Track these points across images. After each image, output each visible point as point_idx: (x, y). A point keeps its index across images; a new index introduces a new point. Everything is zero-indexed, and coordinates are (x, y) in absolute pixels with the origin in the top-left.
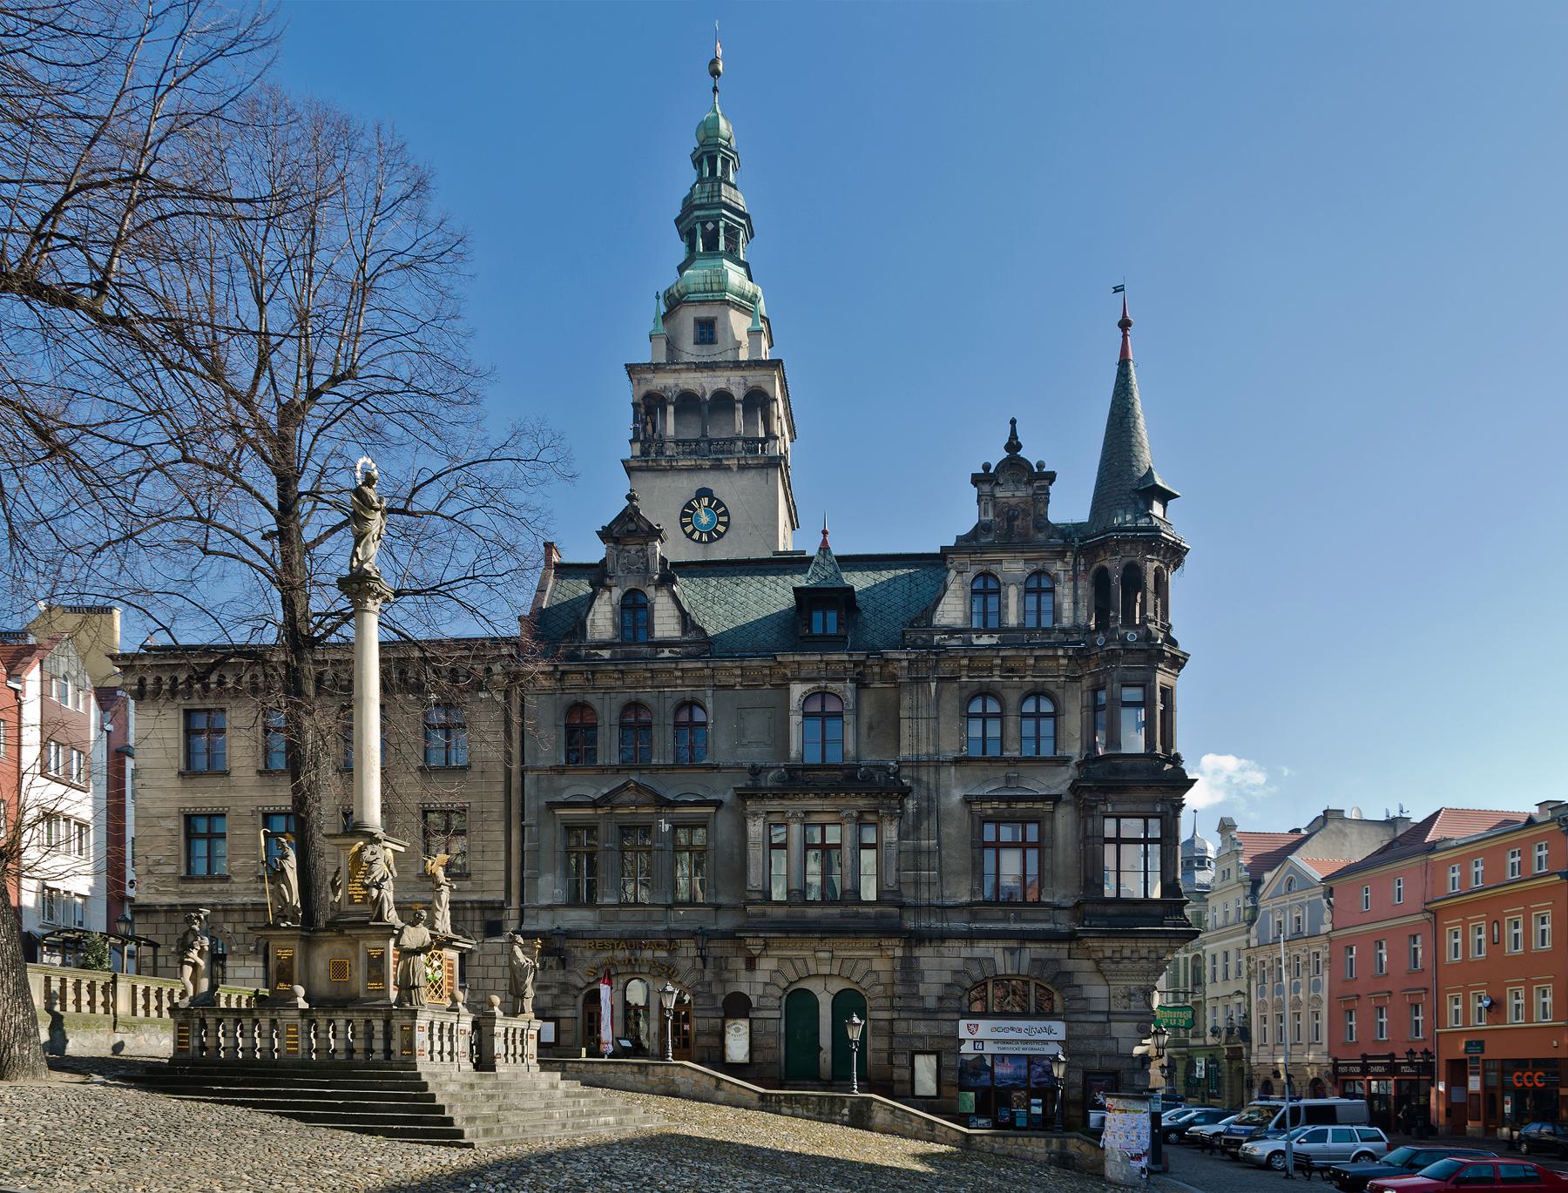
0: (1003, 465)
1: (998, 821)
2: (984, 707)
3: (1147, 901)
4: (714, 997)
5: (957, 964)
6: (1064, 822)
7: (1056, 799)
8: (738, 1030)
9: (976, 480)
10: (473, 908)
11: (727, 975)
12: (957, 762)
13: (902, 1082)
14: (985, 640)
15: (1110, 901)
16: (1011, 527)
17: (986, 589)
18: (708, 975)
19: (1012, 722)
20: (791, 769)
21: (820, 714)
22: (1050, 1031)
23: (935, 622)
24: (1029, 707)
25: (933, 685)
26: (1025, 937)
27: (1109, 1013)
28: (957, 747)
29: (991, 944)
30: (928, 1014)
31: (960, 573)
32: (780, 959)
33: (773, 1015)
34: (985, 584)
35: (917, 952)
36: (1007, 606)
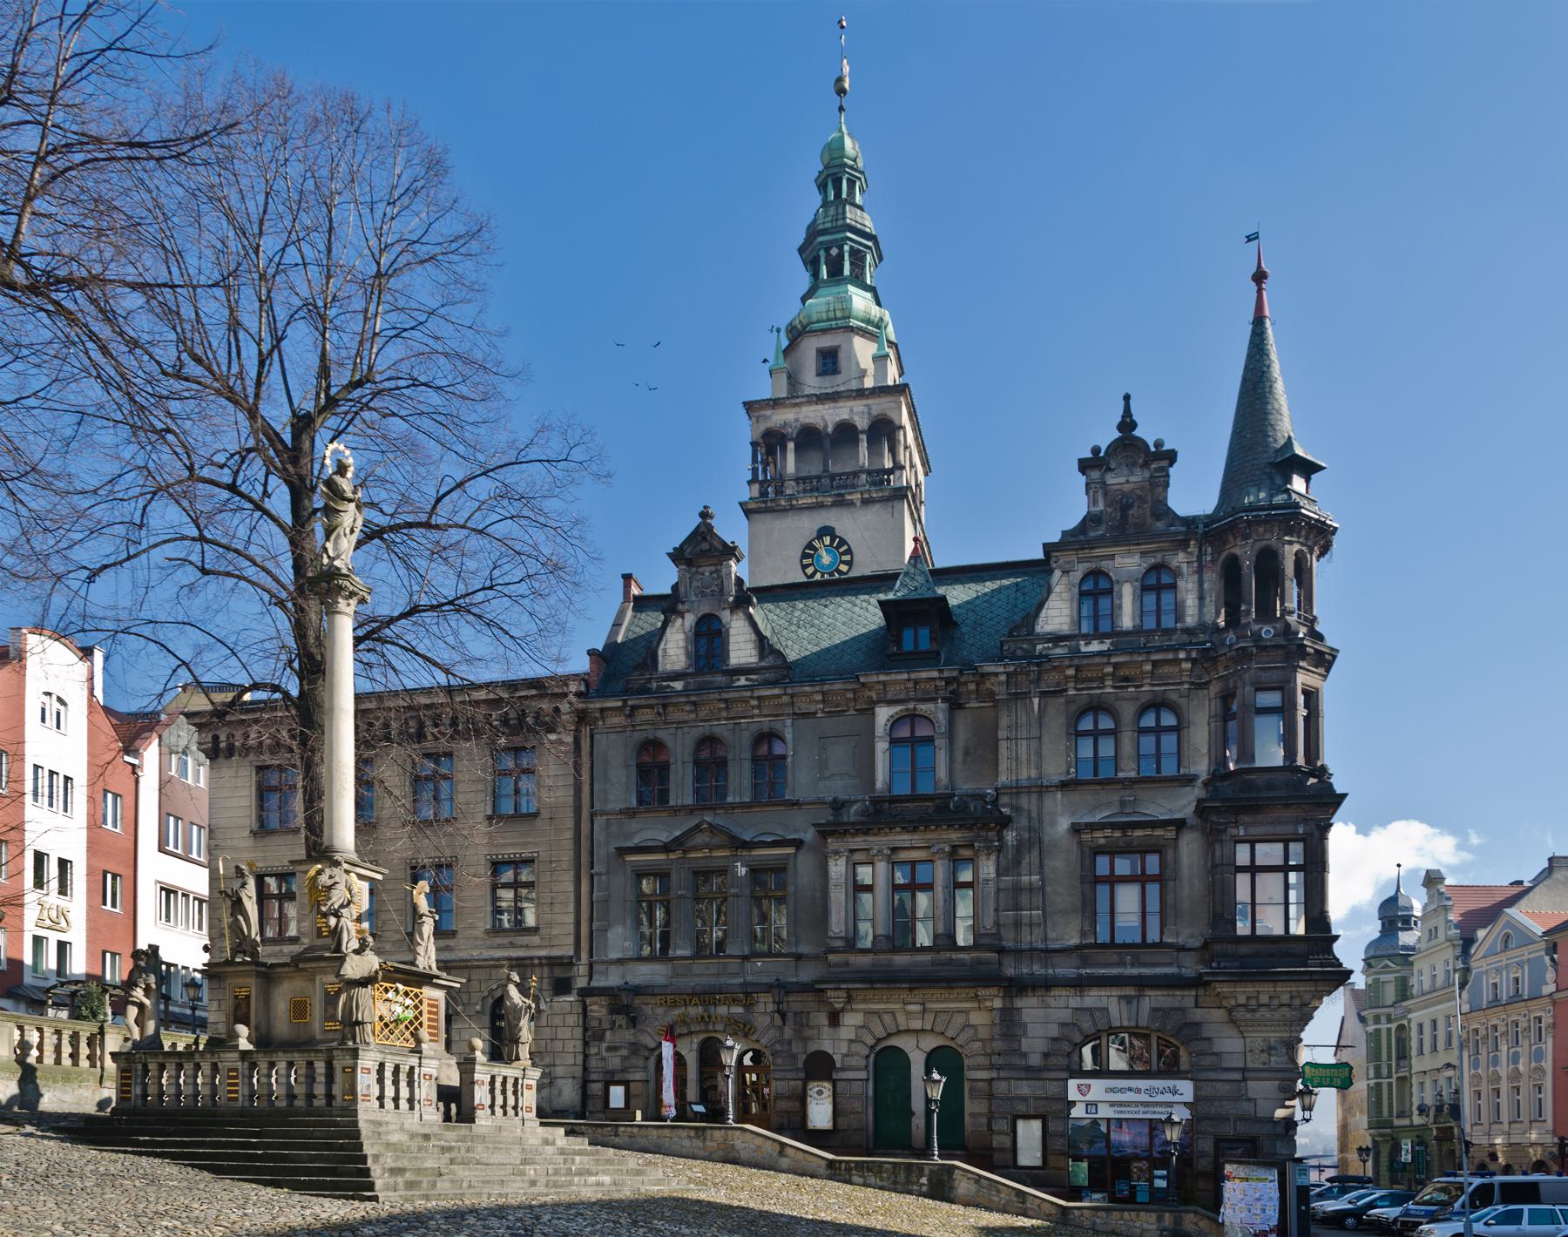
0: (1114, 447)
1: (1113, 851)
2: (1096, 723)
3: (1287, 938)
4: (794, 1057)
5: (1065, 1015)
6: (1189, 849)
7: (1180, 824)
8: (820, 1093)
9: (1084, 466)
10: (541, 965)
11: (809, 1033)
13: (1002, 1150)
14: (1095, 646)
15: (1244, 939)
16: (1124, 517)
17: (1096, 589)
18: (788, 1032)
19: (1127, 739)
20: (877, 801)
21: (910, 738)
22: (1175, 1092)
23: (1038, 629)
24: (1149, 721)
25: (1036, 701)
26: (1143, 983)
27: (1244, 1070)
28: (1064, 768)
29: (1103, 992)
30: (1032, 1073)
31: (1065, 572)
32: (867, 1013)
33: (858, 1075)
34: (1096, 584)
35: (1019, 1003)
36: (1120, 607)
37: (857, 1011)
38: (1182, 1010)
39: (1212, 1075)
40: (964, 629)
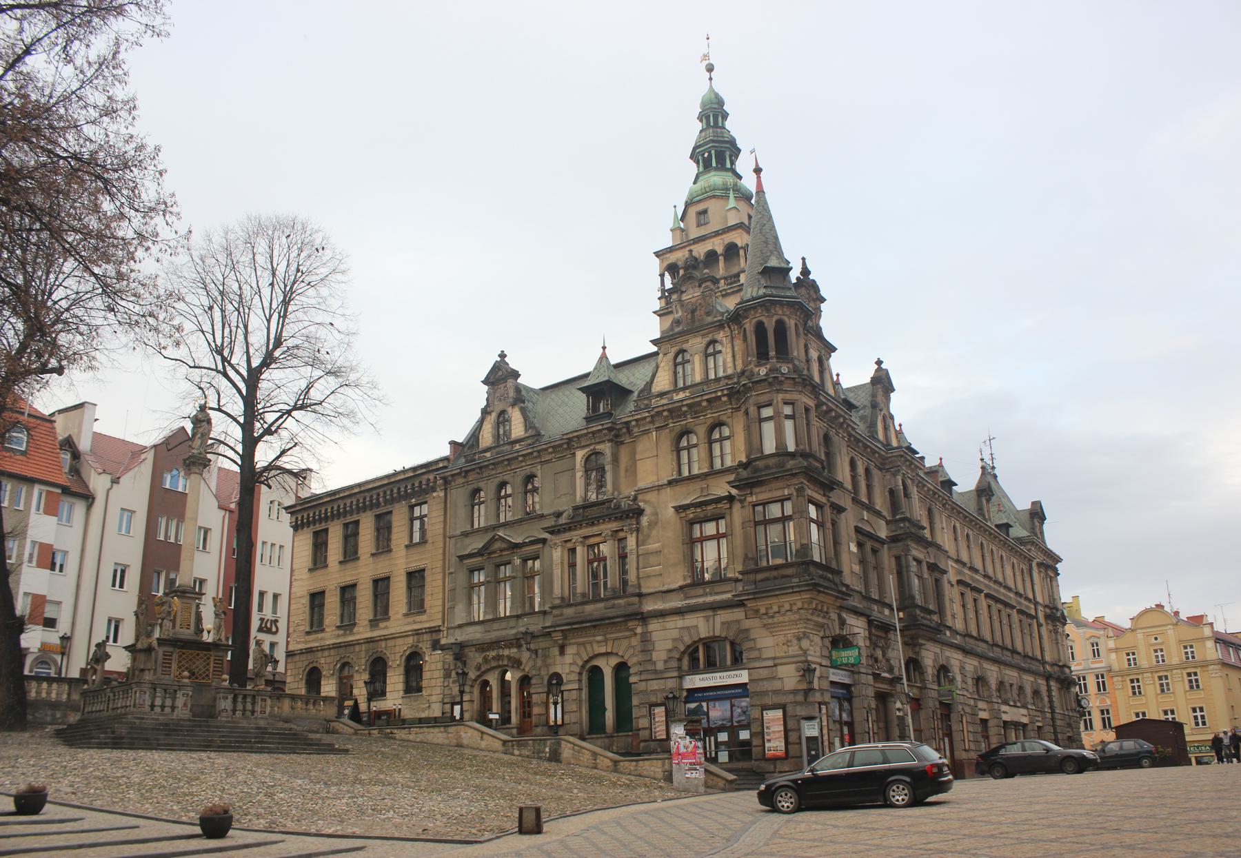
7: (731, 498)
18: (539, 663)
20: (576, 509)
23: (653, 390)
27: (774, 658)
38: (738, 622)
39: (757, 664)
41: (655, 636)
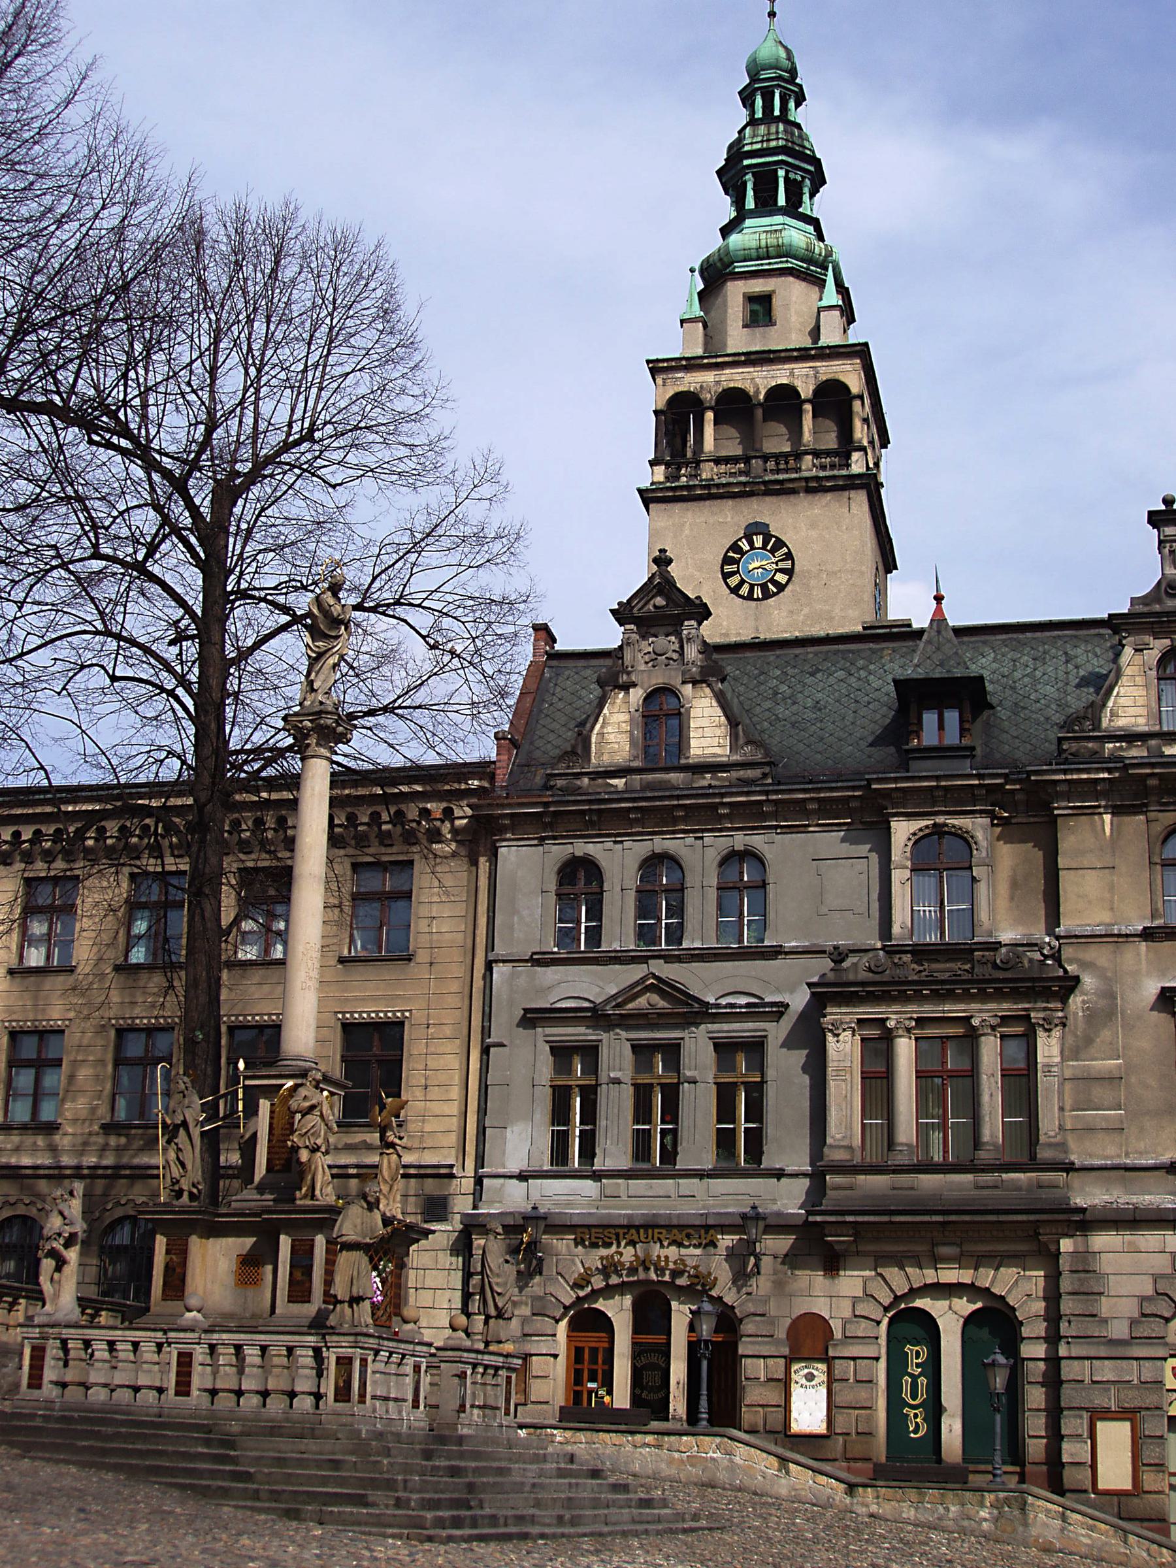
8: (810, 1377)
12: (1148, 935)
30: (1117, 1351)
37: (866, 1254)
40: (1002, 713)
41: (1106, 1264)
